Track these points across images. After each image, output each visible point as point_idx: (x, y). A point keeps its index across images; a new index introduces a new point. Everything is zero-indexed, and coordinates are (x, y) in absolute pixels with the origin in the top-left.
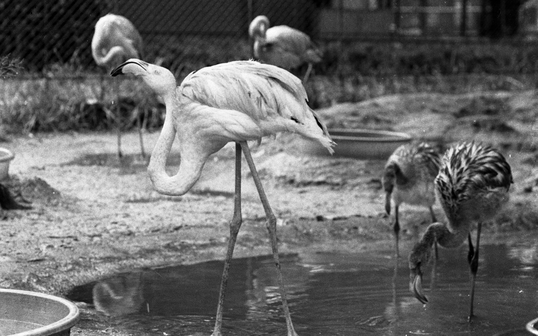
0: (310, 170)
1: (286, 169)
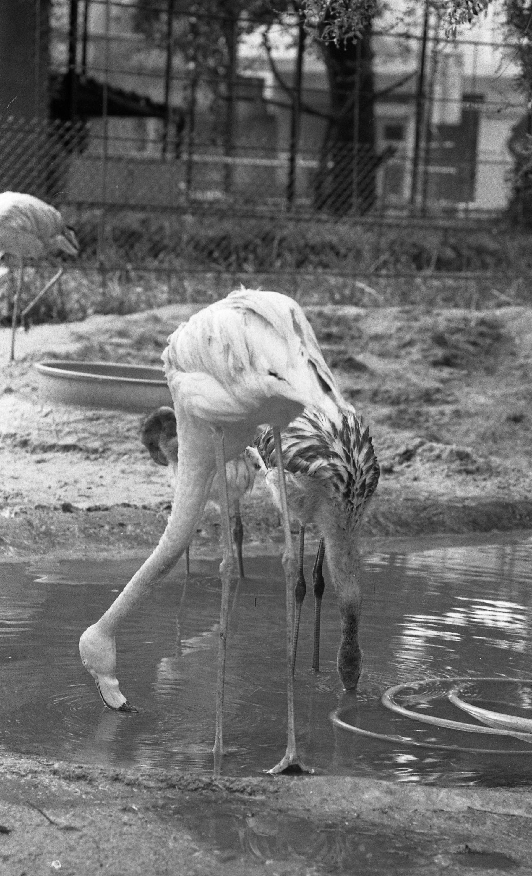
0: (53, 428)
1: (16, 423)
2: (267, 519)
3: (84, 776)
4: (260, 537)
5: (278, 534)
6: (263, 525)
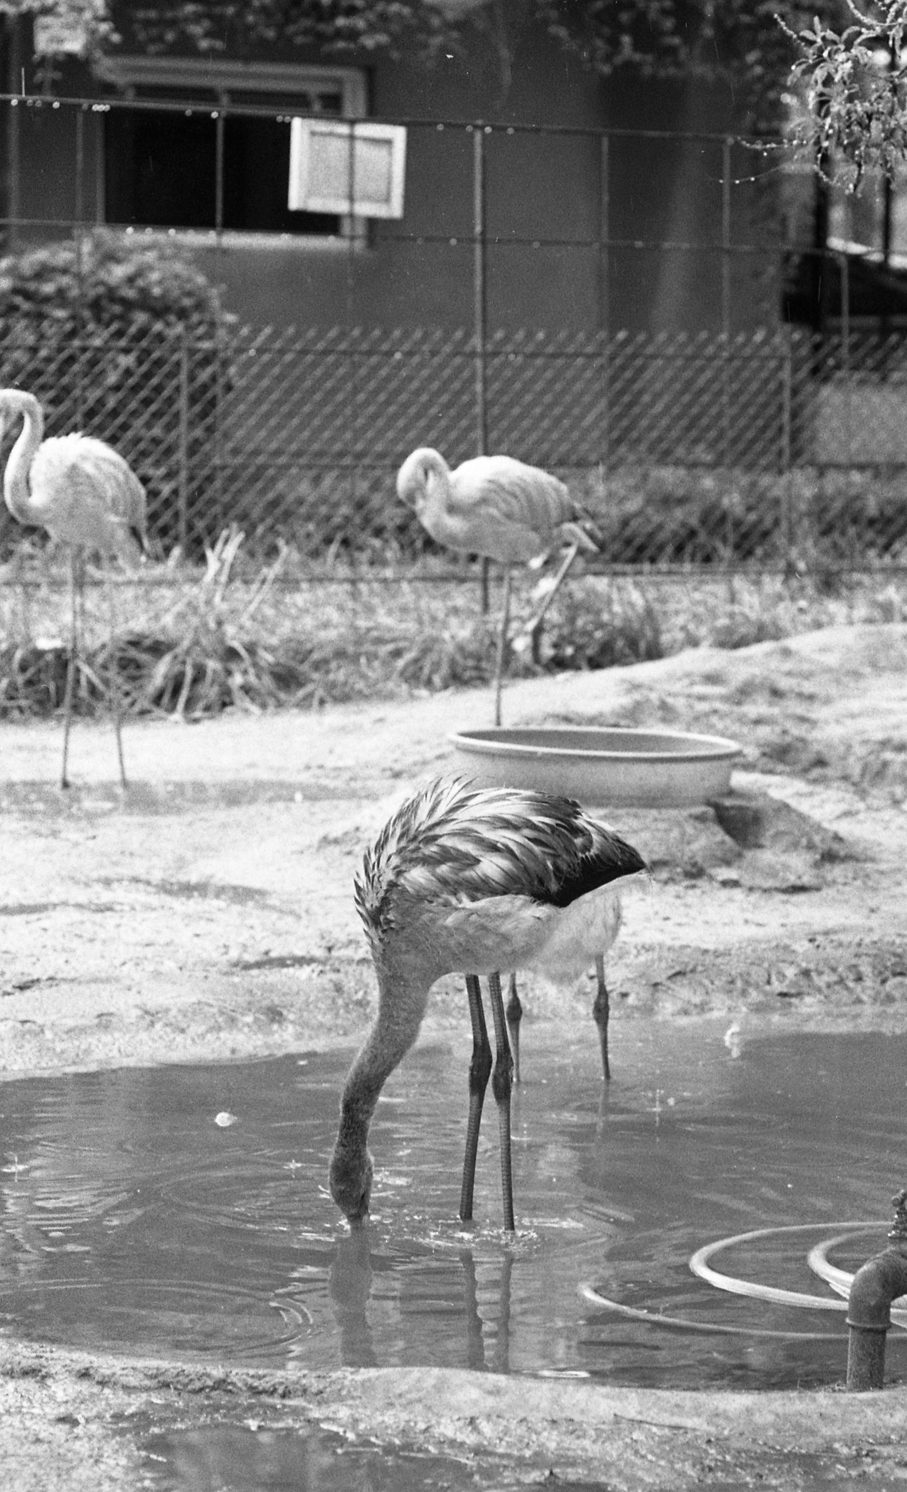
2: (749, 974)
3: (34, 1371)
4: (728, 1002)
5: (761, 998)
6: (739, 984)
